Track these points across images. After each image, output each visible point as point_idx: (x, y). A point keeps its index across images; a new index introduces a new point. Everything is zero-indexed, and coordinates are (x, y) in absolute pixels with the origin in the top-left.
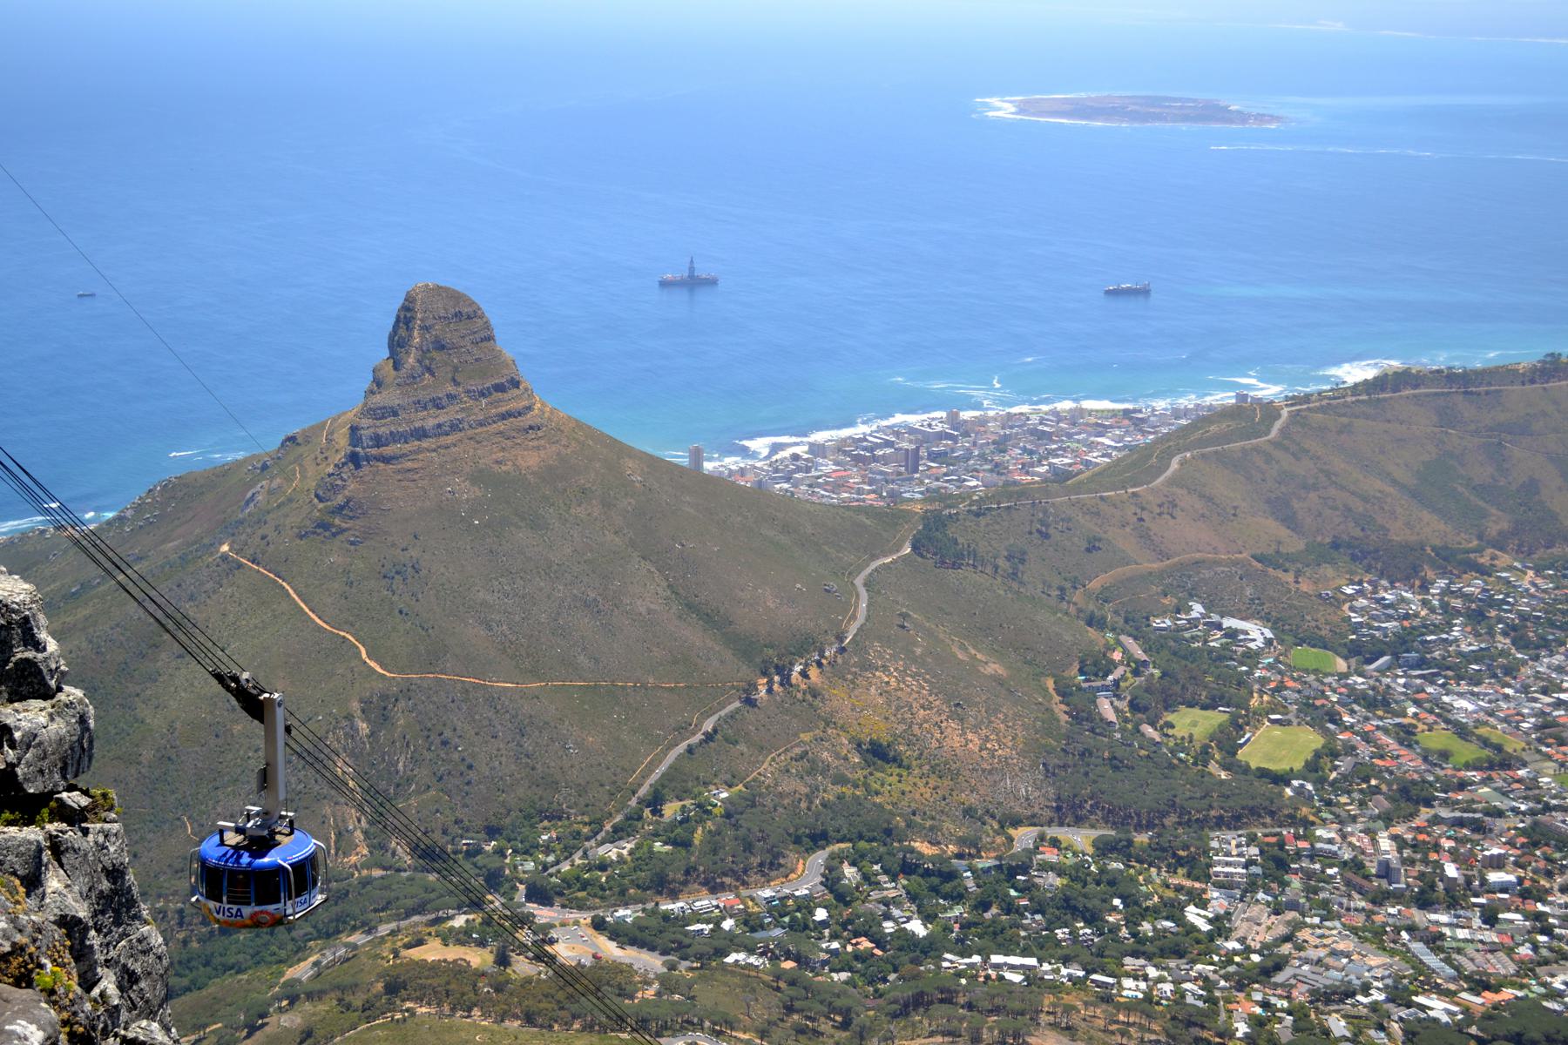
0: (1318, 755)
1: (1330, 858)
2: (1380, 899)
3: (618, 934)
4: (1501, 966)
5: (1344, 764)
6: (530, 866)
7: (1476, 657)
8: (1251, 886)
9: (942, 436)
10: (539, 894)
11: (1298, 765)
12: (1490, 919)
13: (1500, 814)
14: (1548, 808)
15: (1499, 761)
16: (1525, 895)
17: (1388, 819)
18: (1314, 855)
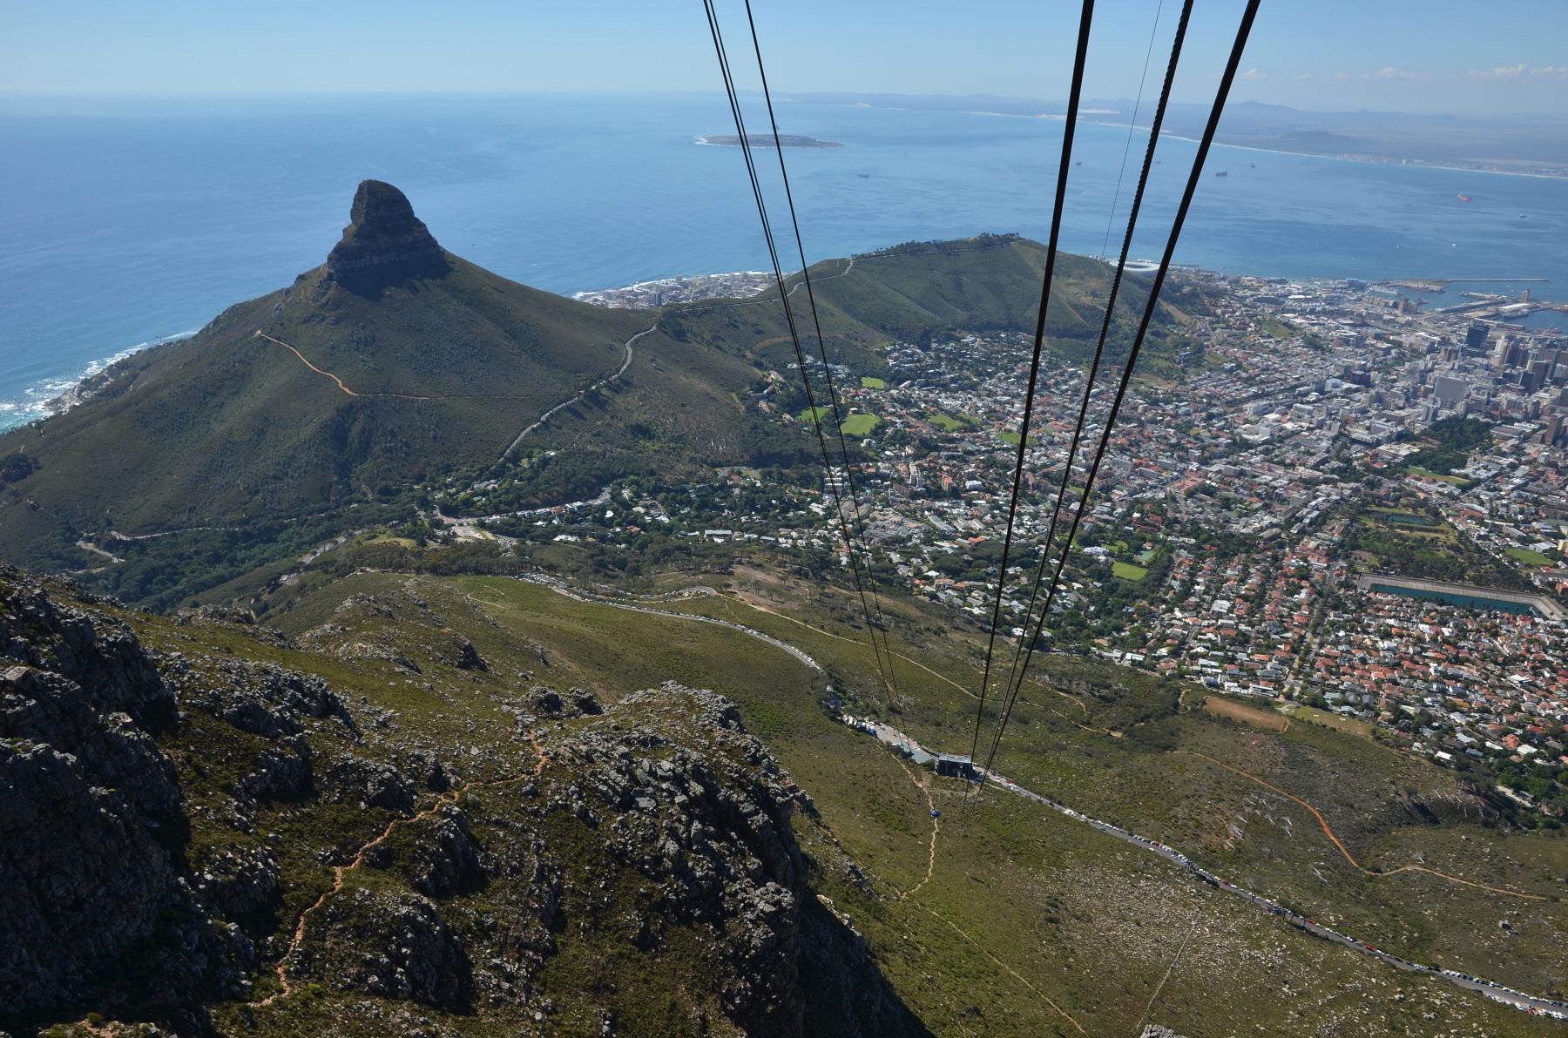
0: (878, 427)
1: (884, 477)
2: (915, 496)
3: (496, 529)
4: (976, 525)
5: (890, 431)
6: (441, 495)
7: (953, 380)
8: (844, 493)
9: (672, 289)
10: (449, 511)
11: (867, 432)
12: (970, 504)
13: (971, 453)
14: (994, 450)
15: (973, 429)
16: (988, 491)
17: (915, 457)
18: (878, 475)
